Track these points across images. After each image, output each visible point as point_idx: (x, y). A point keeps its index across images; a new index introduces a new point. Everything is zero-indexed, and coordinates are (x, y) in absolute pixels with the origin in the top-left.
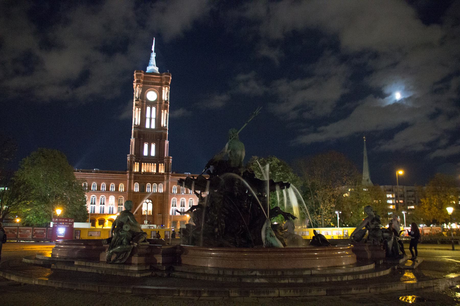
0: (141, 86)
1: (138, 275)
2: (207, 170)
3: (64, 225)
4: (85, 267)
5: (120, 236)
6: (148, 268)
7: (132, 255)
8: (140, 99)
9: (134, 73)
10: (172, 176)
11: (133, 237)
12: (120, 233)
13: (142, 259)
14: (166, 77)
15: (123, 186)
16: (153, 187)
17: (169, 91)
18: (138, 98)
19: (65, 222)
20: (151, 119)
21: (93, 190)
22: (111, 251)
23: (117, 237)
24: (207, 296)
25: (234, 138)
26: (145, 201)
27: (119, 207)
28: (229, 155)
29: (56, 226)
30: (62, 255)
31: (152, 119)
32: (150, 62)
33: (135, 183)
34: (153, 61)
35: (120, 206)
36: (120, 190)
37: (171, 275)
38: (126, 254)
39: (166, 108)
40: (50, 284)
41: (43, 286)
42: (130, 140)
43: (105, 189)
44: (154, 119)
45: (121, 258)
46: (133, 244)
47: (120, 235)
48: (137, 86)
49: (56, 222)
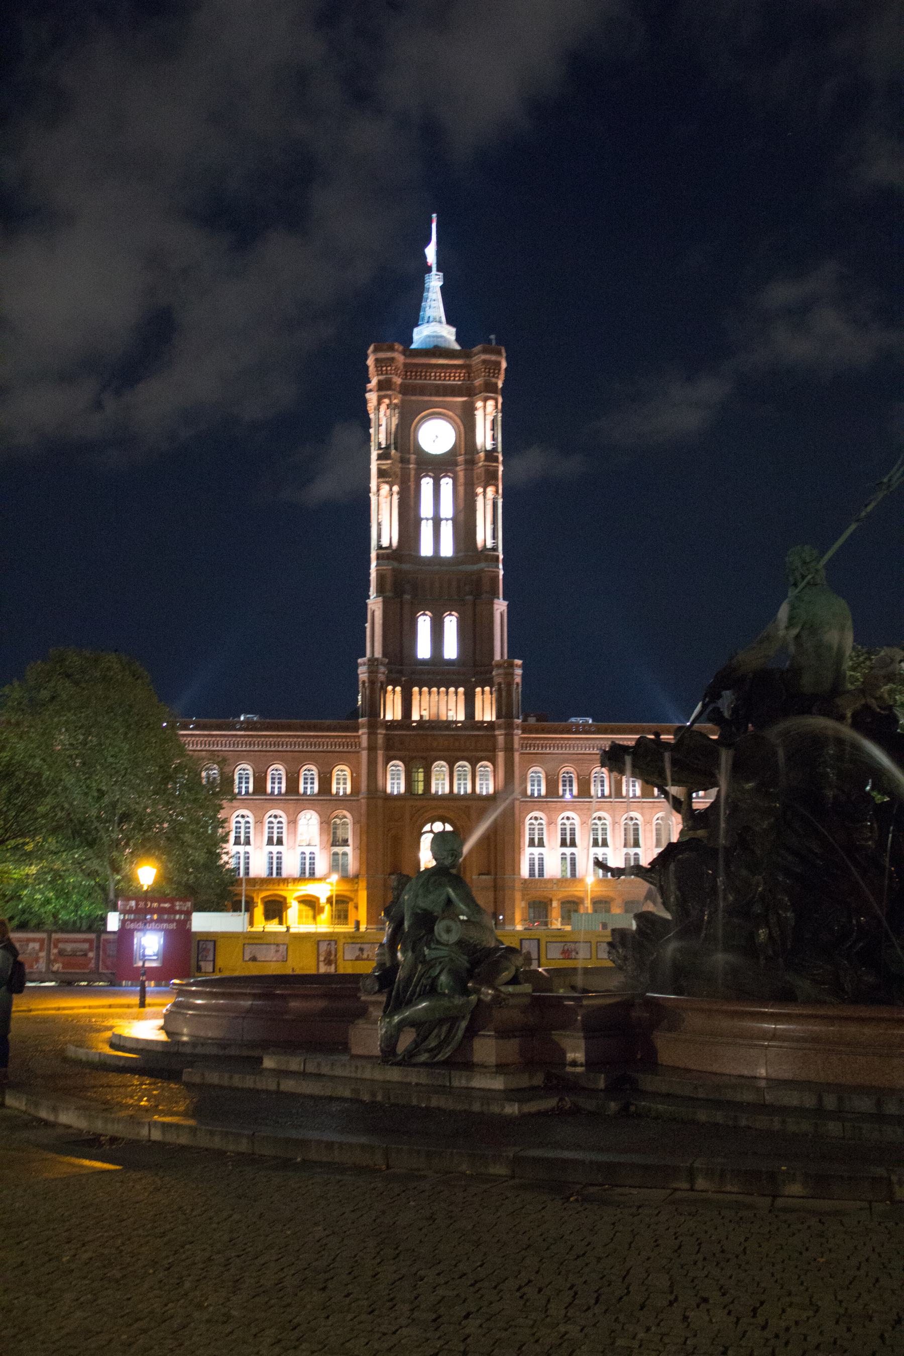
0: (396, 401)
1: (512, 1109)
2: (710, 708)
4: (303, 1075)
5: (424, 962)
6: (539, 1080)
7: (471, 1032)
8: (393, 452)
9: (366, 357)
11: (475, 963)
12: (427, 951)
13: (512, 1046)
14: (484, 362)
15: (348, 773)
16: (455, 774)
17: (500, 415)
18: (388, 447)
19: (160, 911)
20: (437, 521)
22: (396, 1019)
23: (415, 967)
24: (801, 1194)
25: (808, 583)
26: (427, 828)
27: (335, 854)
28: (792, 649)
29: (132, 926)
30: (202, 1034)
31: (443, 523)
33: (391, 763)
35: (340, 850)
36: (338, 789)
37: (633, 1108)
38: (449, 1031)
39: (490, 478)
40: (203, 1141)
41: (183, 1147)
42: (366, 604)
43: (284, 786)
44: (450, 523)
45: (433, 1044)
46: (477, 991)
47: (428, 958)
49: (130, 912)
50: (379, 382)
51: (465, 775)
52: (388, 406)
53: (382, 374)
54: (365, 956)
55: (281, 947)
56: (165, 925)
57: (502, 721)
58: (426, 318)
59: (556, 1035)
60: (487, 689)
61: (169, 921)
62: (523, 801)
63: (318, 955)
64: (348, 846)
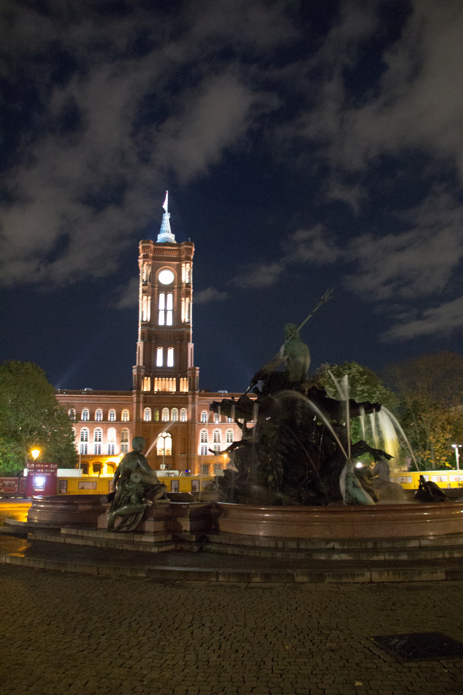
0: (150, 263)
1: (155, 550)
2: (254, 387)
3: (44, 472)
4: (77, 537)
6: (169, 538)
7: (145, 518)
8: (149, 283)
9: (139, 245)
10: (200, 396)
11: (147, 491)
12: (127, 486)
13: (160, 525)
14: (186, 248)
16: (172, 413)
17: (192, 269)
18: (146, 281)
19: (44, 468)
20: (166, 311)
22: (114, 513)
23: (122, 492)
24: (260, 581)
25: (292, 338)
26: (160, 435)
27: (123, 445)
28: (286, 364)
29: (33, 474)
30: (43, 519)
31: (168, 312)
37: (204, 549)
38: (135, 518)
39: (187, 294)
40: (26, 563)
41: (18, 566)
44: (171, 312)
45: (128, 524)
46: (146, 502)
47: (127, 489)
48: (143, 264)
49: (32, 468)
50: (144, 255)
52: (147, 265)
53: (144, 252)
55: (94, 483)
56: (46, 474)
57: (191, 392)
58: (163, 231)
59: (179, 520)
60: (185, 379)
61: (48, 472)
63: (109, 487)
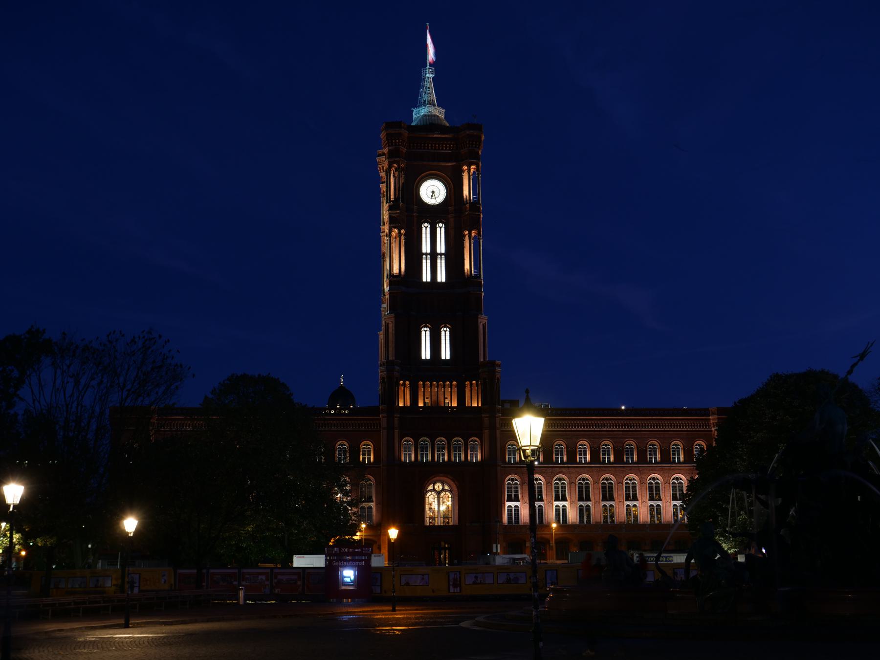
15: (371, 447)
20: (434, 255)
21: (581, 462)
26: (431, 487)
32: (421, 96)
34: (429, 91)
39: (474, 224)
51: (460, 447)
52: (396, 169)
53: (392, 145)
54: (479, 581)
60: (474, 382)
62: (502, 467)
64: (373, 502)
